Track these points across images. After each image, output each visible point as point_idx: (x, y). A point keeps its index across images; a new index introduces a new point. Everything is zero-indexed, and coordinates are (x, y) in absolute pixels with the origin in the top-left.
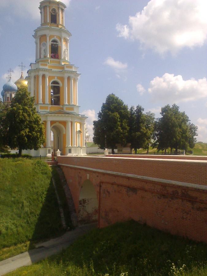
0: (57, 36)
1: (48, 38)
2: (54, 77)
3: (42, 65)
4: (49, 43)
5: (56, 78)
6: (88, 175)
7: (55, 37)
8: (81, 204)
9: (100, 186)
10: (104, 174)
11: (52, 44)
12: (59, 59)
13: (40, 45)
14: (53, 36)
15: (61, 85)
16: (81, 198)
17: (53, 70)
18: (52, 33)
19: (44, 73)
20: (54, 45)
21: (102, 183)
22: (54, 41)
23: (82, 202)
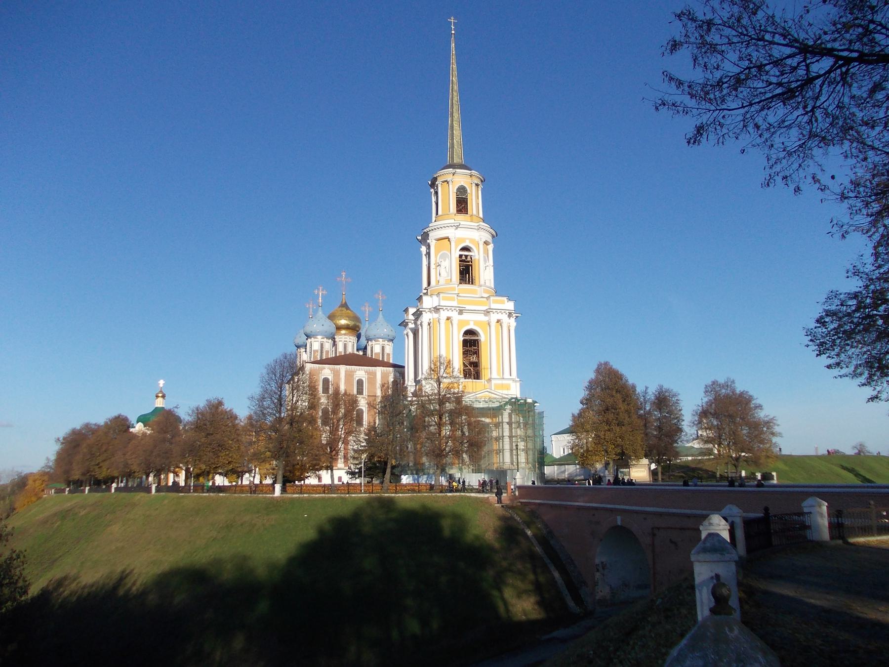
0: (472, 241)
1: (453, 243)
2: (467, 322)
3: (445, 299)
4: (456, 253)
5: (472, 323)
6: (619, 518)
10: (661, 514)
11: (461, 256)
13: (436, 256)
14: (464, 240)
17: (468, 307)
18: (460, 233)
21: (658, 529)
23: (600, 569)
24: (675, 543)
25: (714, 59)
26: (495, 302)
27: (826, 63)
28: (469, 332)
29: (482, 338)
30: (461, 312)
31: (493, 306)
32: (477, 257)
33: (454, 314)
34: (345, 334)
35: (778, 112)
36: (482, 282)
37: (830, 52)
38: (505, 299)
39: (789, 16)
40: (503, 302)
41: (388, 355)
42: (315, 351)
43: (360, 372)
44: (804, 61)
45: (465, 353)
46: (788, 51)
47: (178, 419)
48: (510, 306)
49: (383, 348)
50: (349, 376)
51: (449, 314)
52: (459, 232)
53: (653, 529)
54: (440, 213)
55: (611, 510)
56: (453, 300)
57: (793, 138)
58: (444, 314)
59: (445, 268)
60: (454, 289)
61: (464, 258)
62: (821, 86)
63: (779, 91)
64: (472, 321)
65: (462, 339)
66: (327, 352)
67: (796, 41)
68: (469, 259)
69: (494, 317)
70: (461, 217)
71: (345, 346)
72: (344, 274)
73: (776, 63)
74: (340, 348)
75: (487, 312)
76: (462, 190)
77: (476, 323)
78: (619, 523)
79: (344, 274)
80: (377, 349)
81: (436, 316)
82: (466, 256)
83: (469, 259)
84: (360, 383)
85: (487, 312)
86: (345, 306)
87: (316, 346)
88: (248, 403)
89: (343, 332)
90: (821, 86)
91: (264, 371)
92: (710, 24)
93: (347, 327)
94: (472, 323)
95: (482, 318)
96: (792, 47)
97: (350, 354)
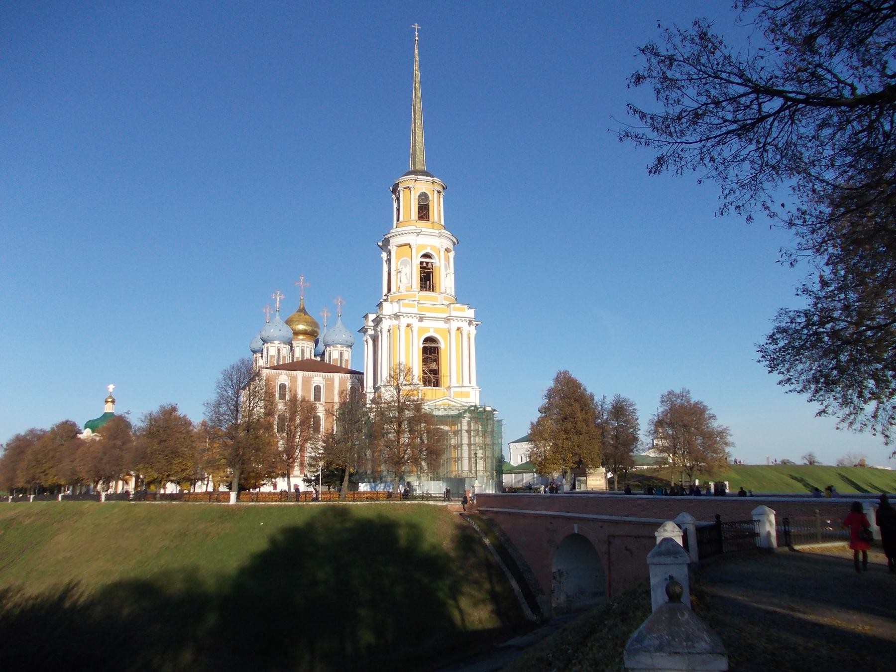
0: (433, 247)
2: (428, 330)
3: (405, 305)
4: (417, 260)
5: (432, 330)
6: (576, 527)
8: (554, 578)
9: (610, 543)
10: (617, 522)
11: (422, 263)
12: (437, 289)
14: (425, 247)
16: (554, 569)
17: (428, 314)
19: (410, 321)
21: (614, 536)
22: (424, 256)
24: (630, 551)
25: (674, 95)
26: (455, 309)
27: (776, 103)
28: (429, 340)
29: (442, 345)
30: (421, 319)
31: (454, 313)
32: (438, 264)
33: (415, 322)
34: (302, 340)
35: (734, 145)
36: (443, 290)
37: (780, 94)
38: (465, 306)
39: (743, 58)
40: (463, 310)
41: (347, 361)
42: (272, 357)
43: (318, 379)
44: (757, 99)
45: (425, 360)
46: (742, 90)
47: (128, 425)
48: (471, 313)
49: (341, 354)
50: (306, 382)
51: (410, 321)
52: (419, 239)
53: (609, 536)
54: (401, 219)
55: (569, 518)
56: (413, 306)
57: (745, 170)
58: (404, 321)
59: (406, 275)
60: (414, 296)
61: (425, 265)
62: (772, 124)
63: (734, 127)
64: (432, 328)
65: (422, 346)
66: (284, 357)
67: (750, 81)
68: (430, 266)
69: (454, 325)
70: (422, 223)
71: (303, 352)
72: (302, 279)
73: (733, 100)
74: (298, 354)
75: (447, 320)
76: (424, 197)
77: (436, 330)
78: (576, 531)
79: (302, 279)
80: (335, 355)
81: (396, 322)
82: (427, 263)
83: (430, 266)
84: (317, 389)
85: (447, 320)
86: (302, 310)
87: (273, 351)
88: (203, 409)
89: (301, 337)
90: (772, 124)
91: (221, 377)
92: (671, 59)
93: (305, 333)
94: (432, 330)
95: (442, 325)
96: (746, 86)
97: (307, 360)
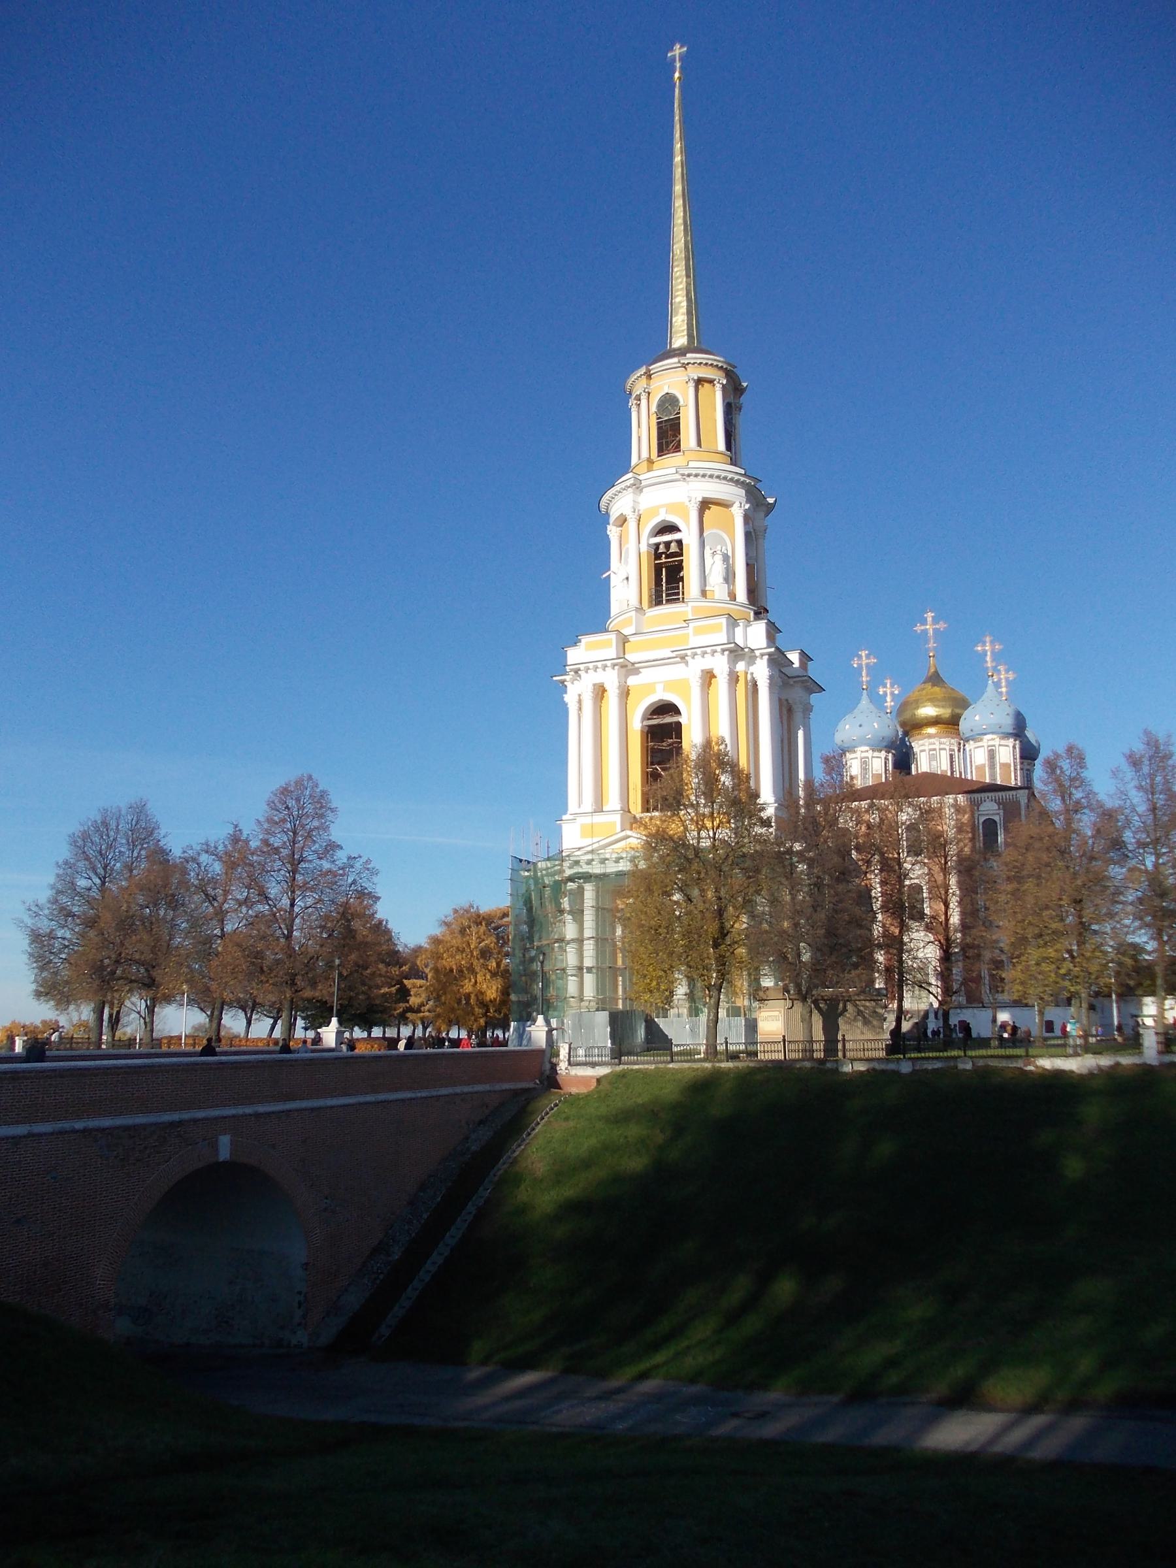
0: (671, 508)
2: (650, 687)
5: (659, 687)
7: (662, 511)
14: (654, 511)
15: (683, 719)
20: (662, 549)
30: (628, 669)
31: (695, 641)
41: (1005, 766)
49: (992, 755)
52: (673, 495)
65: (636, 725)
68: (674, 548)
69: (698, 665)
72: (929, 616)
76: (669, 402)
77: (668, 685)
79: (929, 616)
83: (674, 548)
86: (935, 679)
89: (932, 730)
93: (935, 722)
94: (659, 687)
97: (925, 774)
